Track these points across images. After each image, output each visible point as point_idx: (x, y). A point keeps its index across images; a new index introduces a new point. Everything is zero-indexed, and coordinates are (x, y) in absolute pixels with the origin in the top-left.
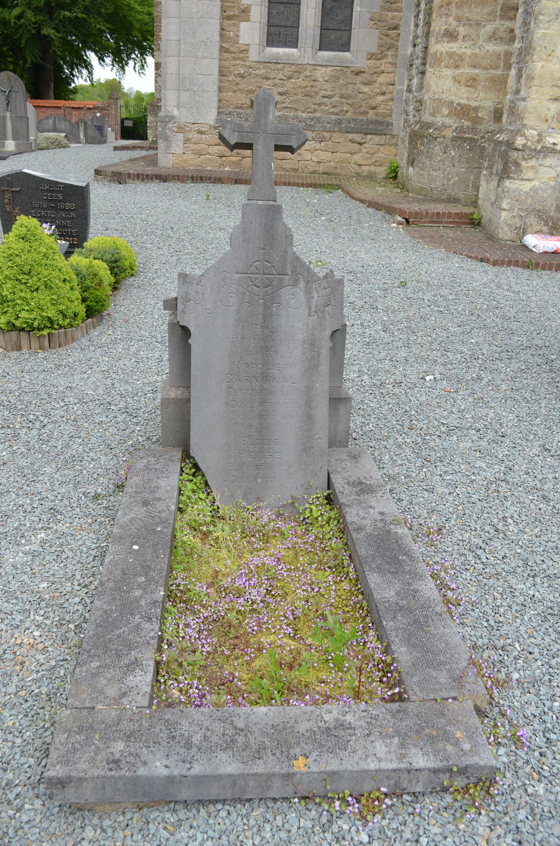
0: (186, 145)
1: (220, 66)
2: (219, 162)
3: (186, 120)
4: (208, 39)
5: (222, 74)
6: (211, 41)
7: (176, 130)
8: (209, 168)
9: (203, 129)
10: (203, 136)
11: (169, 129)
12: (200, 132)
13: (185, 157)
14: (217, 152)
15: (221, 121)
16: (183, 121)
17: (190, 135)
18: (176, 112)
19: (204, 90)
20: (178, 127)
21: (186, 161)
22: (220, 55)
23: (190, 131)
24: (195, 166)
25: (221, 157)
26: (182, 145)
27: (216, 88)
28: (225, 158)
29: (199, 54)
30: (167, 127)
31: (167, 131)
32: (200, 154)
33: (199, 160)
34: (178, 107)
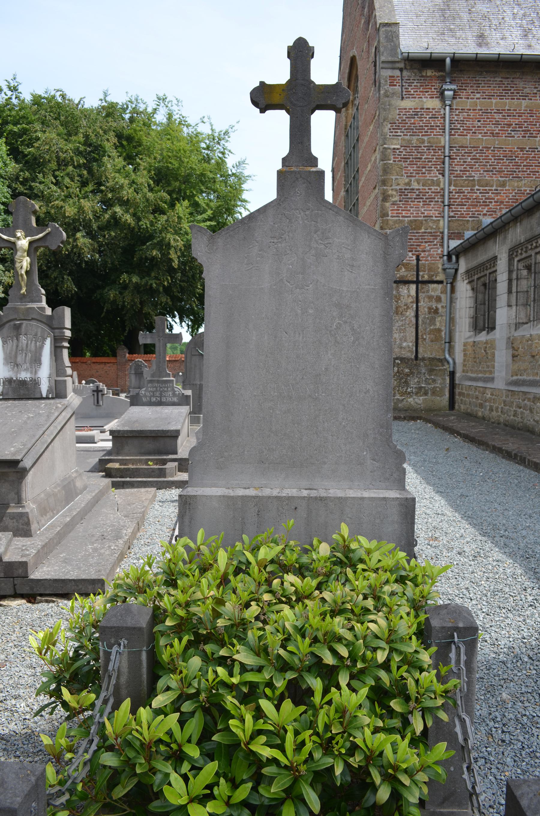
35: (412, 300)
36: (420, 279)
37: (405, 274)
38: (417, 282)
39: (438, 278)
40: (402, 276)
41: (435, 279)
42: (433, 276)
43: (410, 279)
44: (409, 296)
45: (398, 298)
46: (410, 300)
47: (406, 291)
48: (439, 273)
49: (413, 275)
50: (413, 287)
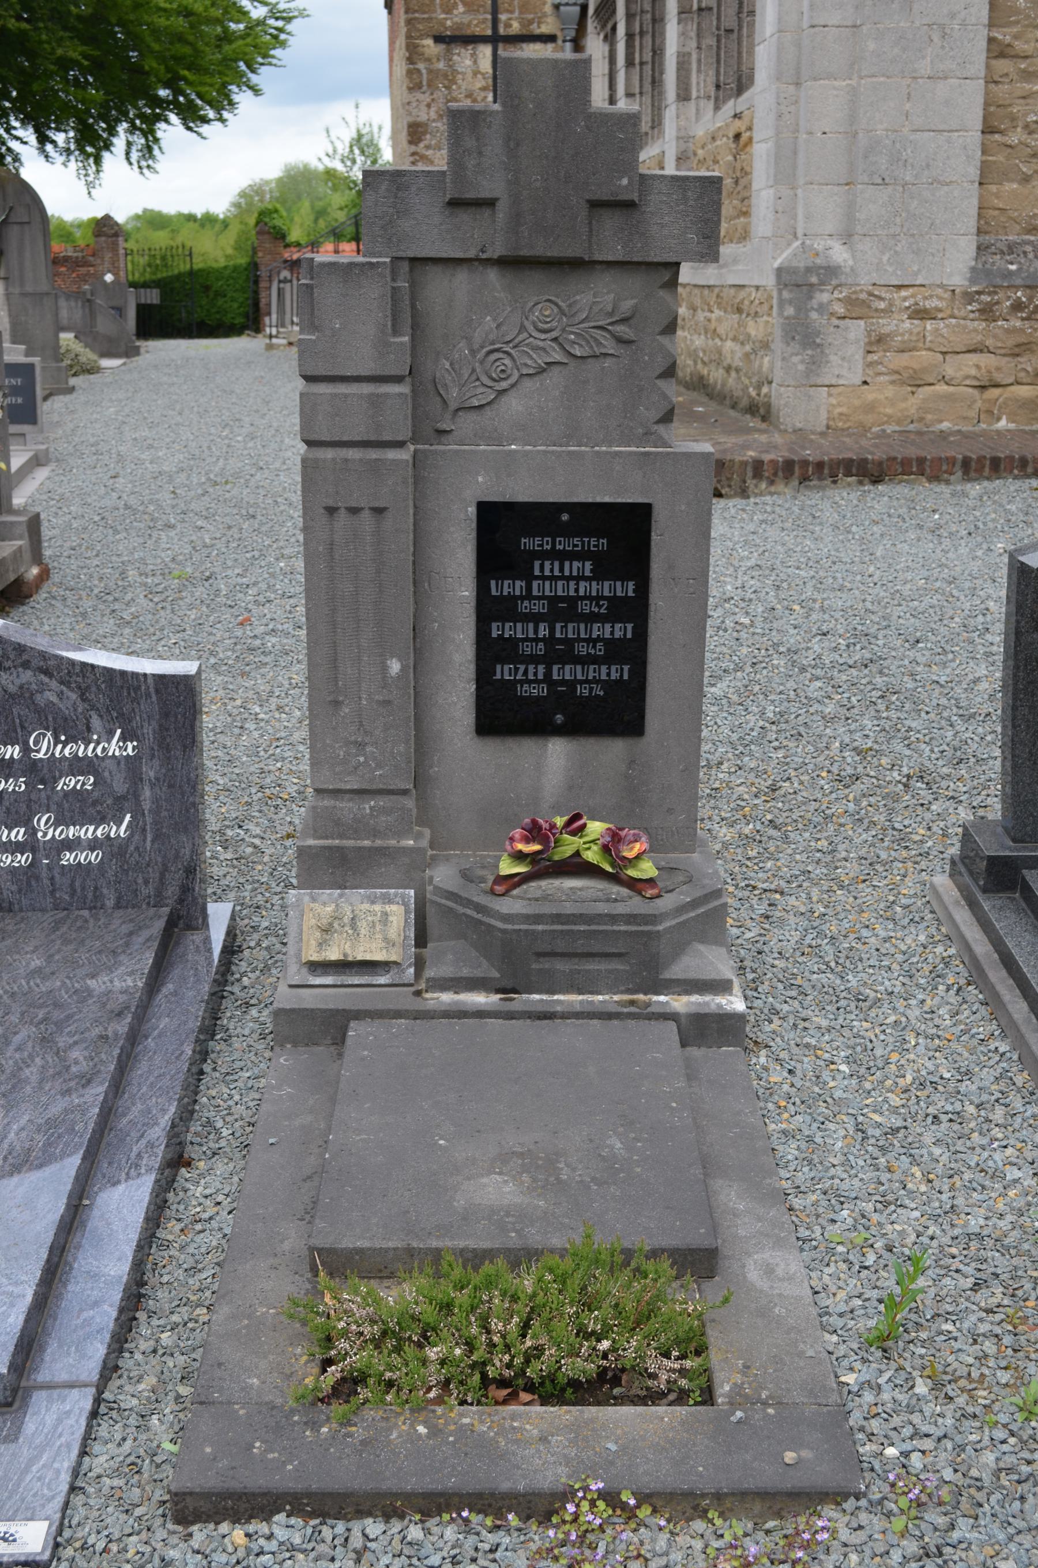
0: (874, 357)
1: (987, 104)
2: (979, 404)
3: (875, 277)
4: (953, 16)
5: (988, 129)
6: (963, 24)
7: (841, 310)
8: (945, 425)
9: (929, 304)
10: (929, 325)
11: (821, 308)
12: (920, 314)
13: (870, 395)
14: (973, 372)
15: (988, 273)
16: (864, 281)
17: (887, 325)
18: (840, 254)
19: (935, 180)
20: (850, 301)
21: (870, 408)
22: (988, 67)
23: (888, 312)
24: (899, 422)
25: (983, 388)
26: (859, 356)
27: (974, 173)
28: (996, 392)
29: (924, 67)
30: (814, 303)
31: (814, 315)
32: (915, 381)
33: (912, 404)
34: (847, 237)
35: (483, 83)
36: (502, 31)
37: (466, 19)
38: (495, 40)
39: (545, 29)
40: (459, 26)
41: (537, 32)
42: (531, 22)
43: (478, 31)
44: (476, 73)
45: (450, 78)
46: (479, 83)
47: (468, 62)
48: (545, 15)
49: (484, 21)
50: (485, 52)
